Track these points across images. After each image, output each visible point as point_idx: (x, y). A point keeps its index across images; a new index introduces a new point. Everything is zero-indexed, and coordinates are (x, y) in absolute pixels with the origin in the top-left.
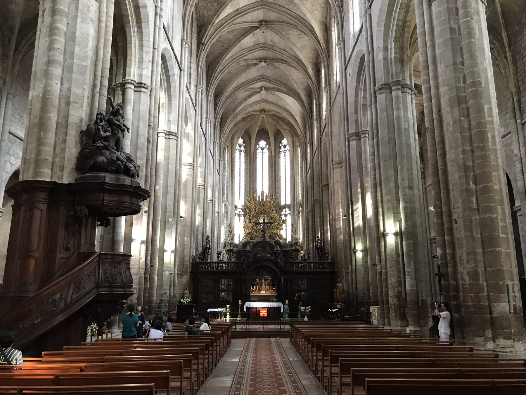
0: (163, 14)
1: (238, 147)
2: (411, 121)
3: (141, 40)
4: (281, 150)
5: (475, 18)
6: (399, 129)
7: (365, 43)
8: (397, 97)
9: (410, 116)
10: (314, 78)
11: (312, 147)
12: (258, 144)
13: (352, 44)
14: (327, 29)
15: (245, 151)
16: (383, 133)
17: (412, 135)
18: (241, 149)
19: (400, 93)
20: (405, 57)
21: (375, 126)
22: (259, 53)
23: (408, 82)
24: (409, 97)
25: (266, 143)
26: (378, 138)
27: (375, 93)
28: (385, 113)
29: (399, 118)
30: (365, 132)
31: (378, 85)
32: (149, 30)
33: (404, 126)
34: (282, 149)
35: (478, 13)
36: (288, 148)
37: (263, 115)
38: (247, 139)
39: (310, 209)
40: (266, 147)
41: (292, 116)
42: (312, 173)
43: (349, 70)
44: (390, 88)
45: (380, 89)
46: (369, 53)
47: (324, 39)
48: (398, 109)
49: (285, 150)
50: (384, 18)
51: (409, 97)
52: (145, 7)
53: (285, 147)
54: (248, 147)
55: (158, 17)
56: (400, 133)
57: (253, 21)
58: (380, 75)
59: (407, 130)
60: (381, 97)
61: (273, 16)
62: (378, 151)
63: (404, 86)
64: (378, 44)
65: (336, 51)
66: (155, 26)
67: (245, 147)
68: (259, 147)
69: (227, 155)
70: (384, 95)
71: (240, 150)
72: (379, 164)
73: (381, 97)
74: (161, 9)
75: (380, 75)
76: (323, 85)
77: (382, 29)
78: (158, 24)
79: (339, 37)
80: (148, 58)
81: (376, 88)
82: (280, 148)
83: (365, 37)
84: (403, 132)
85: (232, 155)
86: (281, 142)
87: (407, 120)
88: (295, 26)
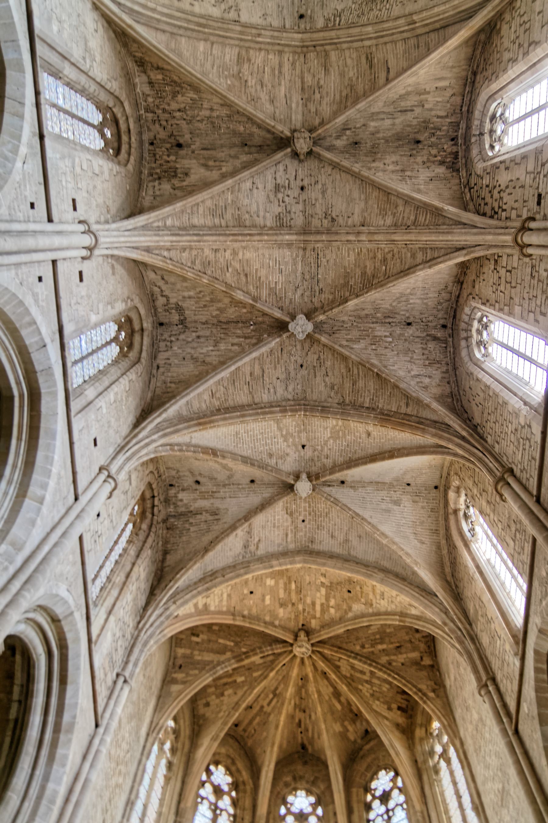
1: (207, 791)
4: (372, 816)
12: (285, 803)
15: (235, 816)
18: (221, 804)
25: (312, 799)
34: (378, 808)
38: (245, 775)
40: (314, 813)
49: (388, 811)
53: (385, 798)
54: (248, 803)
67: (235, 803)
68: (289, 812)
69: (163, 794)
71: (216, 805)
82: (368, 807)
85: (179, 802)
86: (367, 789)
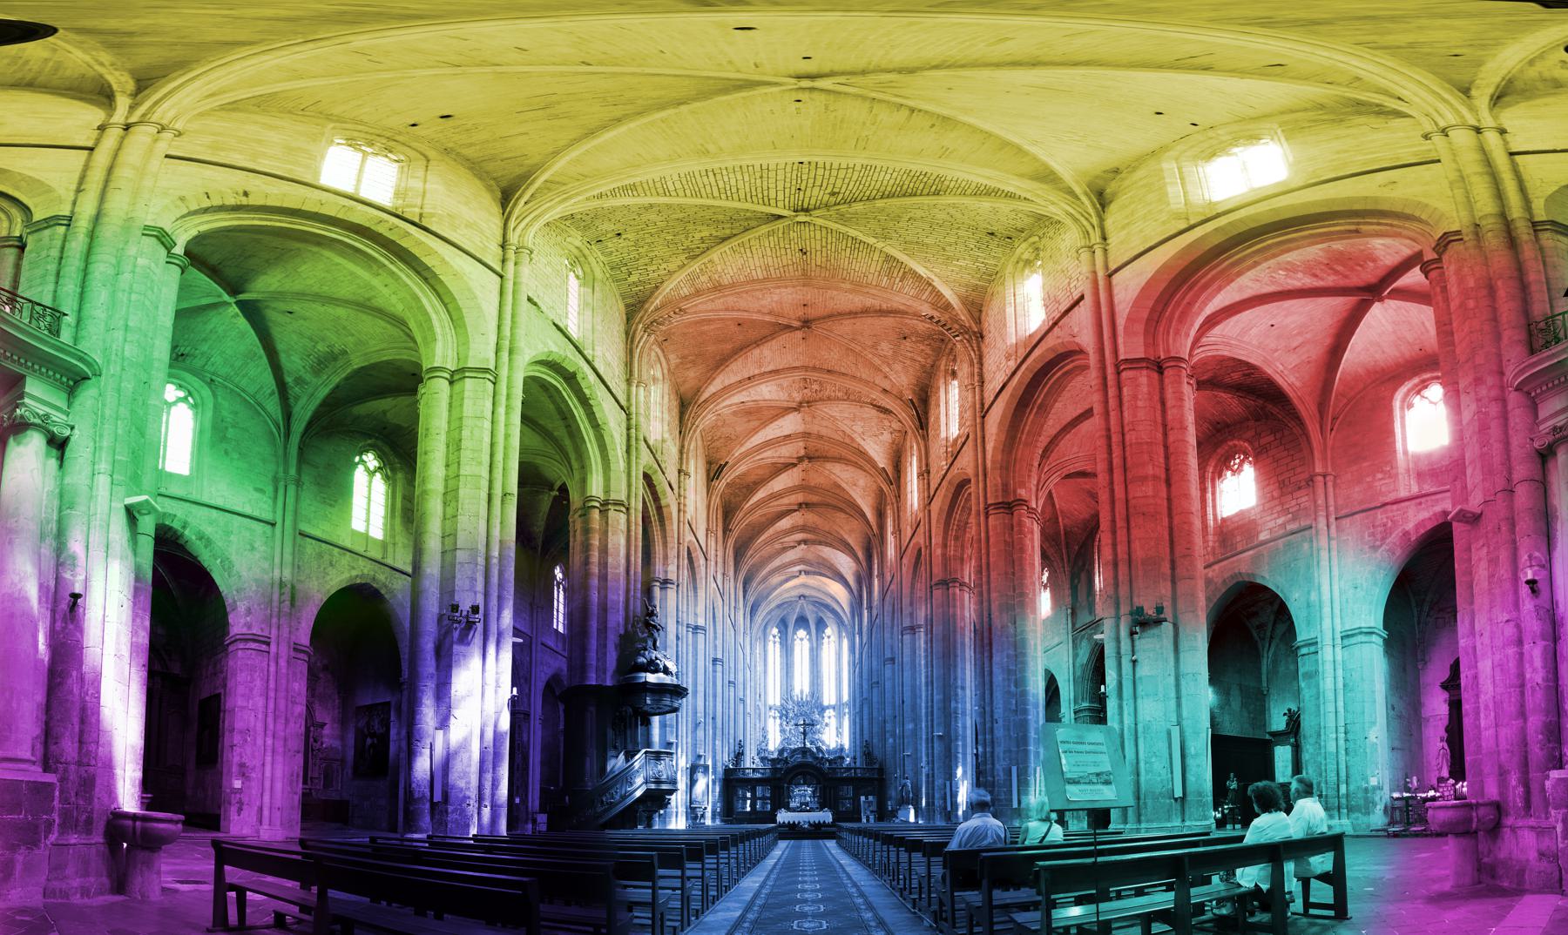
0: (687, 509)
2: (967, 621)
3: (664, 537)
5: (1029, 536)
6: (955, 627)
7: (922, 536)
8: (954, 594)
9: (967, 615)
10: (864, 564)
11: (861, 639)
13: (909, 532)
14: (881, 515)
16: (938, 629)
17: (967, 633)
19: (957, 591)
20: (965, 556)
21: (930, 622)
22: (800, 536)
23: (967, 580)
24: (967, 596)
26: (932, 634)
27: (931, 587)
28: (941, 610)
29: (954, 615)
30: (920, 627)
31: (935, 580)
32: (673, 527)
33: (959, 624)
35: (1032, 533)
36: (832, 638)
37: (802, 601)
39: (857, 710)
41: (838, 602)
42: (861, 668)
43: (905, 561)
44: (947, 584)
45: (936, 584)
46: (926, 547)
47: (877, 524)
48: (954, 606)
50: (944, 517)
51: (967, 596)
52: (668, 506)
55: (682, 513)
56: (955, 631)
57: (790, 504)
58: (937, 570)
59: (963, 629)
60: (937, 593)
61: (814, 499)
62: (932, 647)
63: (962, 584)
64: (936, 539)
65: (890, 540)
66: (679, 522)
70: (940, 591)
72: (932, 661)
73: (937, 593)
74: (685, 505)
75: (937, 570)
76: (876, 573)
77: (942, 526)
78: (682, 519)
79: (894, 527)
80: (672, 553)
81: (933, 583)
83: (922, 531)
84: (959, 630)
87: (963, 618)
88: (841, 510)
